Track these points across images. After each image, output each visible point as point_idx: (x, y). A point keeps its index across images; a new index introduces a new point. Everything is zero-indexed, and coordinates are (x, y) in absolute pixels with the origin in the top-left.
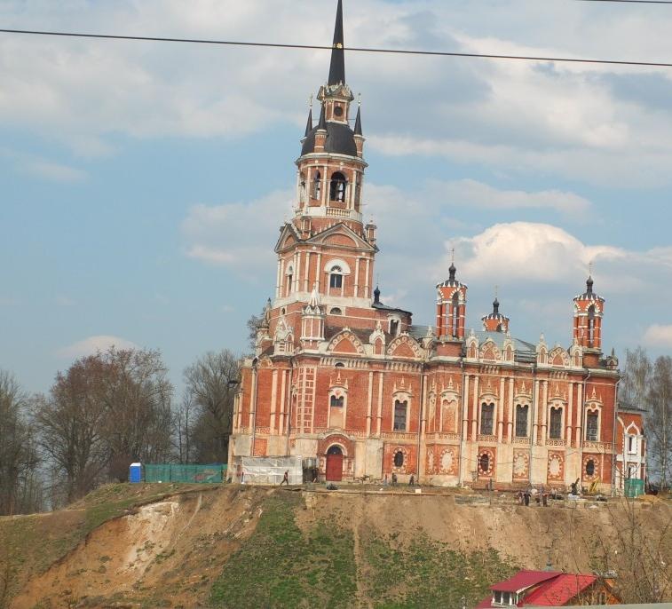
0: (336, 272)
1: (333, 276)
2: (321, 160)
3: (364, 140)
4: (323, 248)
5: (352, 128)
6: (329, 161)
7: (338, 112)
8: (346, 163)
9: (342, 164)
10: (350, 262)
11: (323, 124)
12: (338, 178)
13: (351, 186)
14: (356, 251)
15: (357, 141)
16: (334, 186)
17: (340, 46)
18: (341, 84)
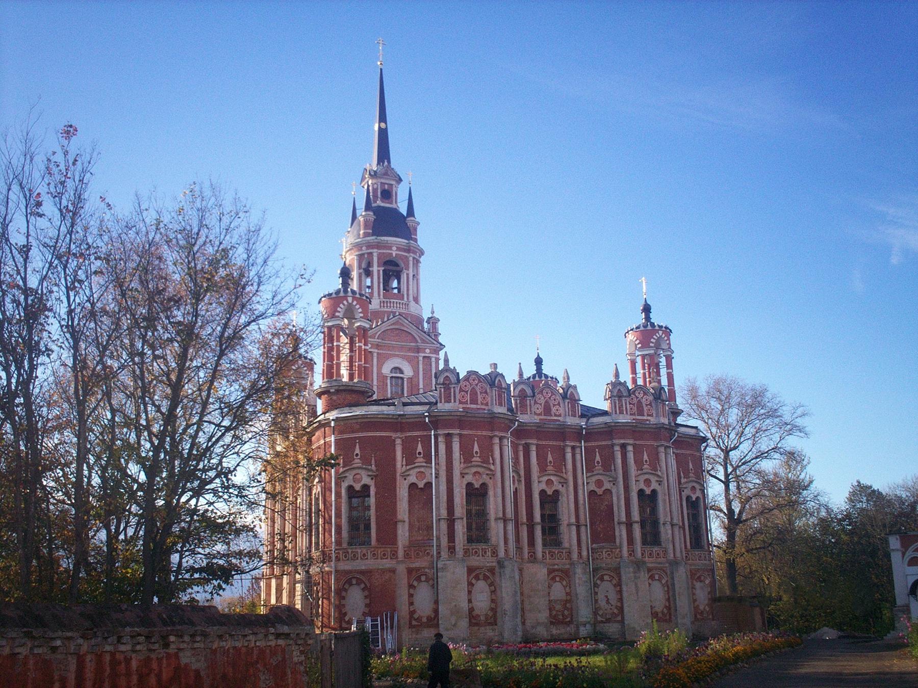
1: (392, 377)
2: (370, 246)
3: (418, 224)
4: (378, 346)
5: (405, 213)
6: (378, 246)
7: (387, 194)
8: (398, 249)
9: (394, 248)
10: (414, 362)
12: (393, 270)
13: (408, 274)
14: (418, 350)
15: (410, 224)
17: (383, 125)
18: (386, 163)
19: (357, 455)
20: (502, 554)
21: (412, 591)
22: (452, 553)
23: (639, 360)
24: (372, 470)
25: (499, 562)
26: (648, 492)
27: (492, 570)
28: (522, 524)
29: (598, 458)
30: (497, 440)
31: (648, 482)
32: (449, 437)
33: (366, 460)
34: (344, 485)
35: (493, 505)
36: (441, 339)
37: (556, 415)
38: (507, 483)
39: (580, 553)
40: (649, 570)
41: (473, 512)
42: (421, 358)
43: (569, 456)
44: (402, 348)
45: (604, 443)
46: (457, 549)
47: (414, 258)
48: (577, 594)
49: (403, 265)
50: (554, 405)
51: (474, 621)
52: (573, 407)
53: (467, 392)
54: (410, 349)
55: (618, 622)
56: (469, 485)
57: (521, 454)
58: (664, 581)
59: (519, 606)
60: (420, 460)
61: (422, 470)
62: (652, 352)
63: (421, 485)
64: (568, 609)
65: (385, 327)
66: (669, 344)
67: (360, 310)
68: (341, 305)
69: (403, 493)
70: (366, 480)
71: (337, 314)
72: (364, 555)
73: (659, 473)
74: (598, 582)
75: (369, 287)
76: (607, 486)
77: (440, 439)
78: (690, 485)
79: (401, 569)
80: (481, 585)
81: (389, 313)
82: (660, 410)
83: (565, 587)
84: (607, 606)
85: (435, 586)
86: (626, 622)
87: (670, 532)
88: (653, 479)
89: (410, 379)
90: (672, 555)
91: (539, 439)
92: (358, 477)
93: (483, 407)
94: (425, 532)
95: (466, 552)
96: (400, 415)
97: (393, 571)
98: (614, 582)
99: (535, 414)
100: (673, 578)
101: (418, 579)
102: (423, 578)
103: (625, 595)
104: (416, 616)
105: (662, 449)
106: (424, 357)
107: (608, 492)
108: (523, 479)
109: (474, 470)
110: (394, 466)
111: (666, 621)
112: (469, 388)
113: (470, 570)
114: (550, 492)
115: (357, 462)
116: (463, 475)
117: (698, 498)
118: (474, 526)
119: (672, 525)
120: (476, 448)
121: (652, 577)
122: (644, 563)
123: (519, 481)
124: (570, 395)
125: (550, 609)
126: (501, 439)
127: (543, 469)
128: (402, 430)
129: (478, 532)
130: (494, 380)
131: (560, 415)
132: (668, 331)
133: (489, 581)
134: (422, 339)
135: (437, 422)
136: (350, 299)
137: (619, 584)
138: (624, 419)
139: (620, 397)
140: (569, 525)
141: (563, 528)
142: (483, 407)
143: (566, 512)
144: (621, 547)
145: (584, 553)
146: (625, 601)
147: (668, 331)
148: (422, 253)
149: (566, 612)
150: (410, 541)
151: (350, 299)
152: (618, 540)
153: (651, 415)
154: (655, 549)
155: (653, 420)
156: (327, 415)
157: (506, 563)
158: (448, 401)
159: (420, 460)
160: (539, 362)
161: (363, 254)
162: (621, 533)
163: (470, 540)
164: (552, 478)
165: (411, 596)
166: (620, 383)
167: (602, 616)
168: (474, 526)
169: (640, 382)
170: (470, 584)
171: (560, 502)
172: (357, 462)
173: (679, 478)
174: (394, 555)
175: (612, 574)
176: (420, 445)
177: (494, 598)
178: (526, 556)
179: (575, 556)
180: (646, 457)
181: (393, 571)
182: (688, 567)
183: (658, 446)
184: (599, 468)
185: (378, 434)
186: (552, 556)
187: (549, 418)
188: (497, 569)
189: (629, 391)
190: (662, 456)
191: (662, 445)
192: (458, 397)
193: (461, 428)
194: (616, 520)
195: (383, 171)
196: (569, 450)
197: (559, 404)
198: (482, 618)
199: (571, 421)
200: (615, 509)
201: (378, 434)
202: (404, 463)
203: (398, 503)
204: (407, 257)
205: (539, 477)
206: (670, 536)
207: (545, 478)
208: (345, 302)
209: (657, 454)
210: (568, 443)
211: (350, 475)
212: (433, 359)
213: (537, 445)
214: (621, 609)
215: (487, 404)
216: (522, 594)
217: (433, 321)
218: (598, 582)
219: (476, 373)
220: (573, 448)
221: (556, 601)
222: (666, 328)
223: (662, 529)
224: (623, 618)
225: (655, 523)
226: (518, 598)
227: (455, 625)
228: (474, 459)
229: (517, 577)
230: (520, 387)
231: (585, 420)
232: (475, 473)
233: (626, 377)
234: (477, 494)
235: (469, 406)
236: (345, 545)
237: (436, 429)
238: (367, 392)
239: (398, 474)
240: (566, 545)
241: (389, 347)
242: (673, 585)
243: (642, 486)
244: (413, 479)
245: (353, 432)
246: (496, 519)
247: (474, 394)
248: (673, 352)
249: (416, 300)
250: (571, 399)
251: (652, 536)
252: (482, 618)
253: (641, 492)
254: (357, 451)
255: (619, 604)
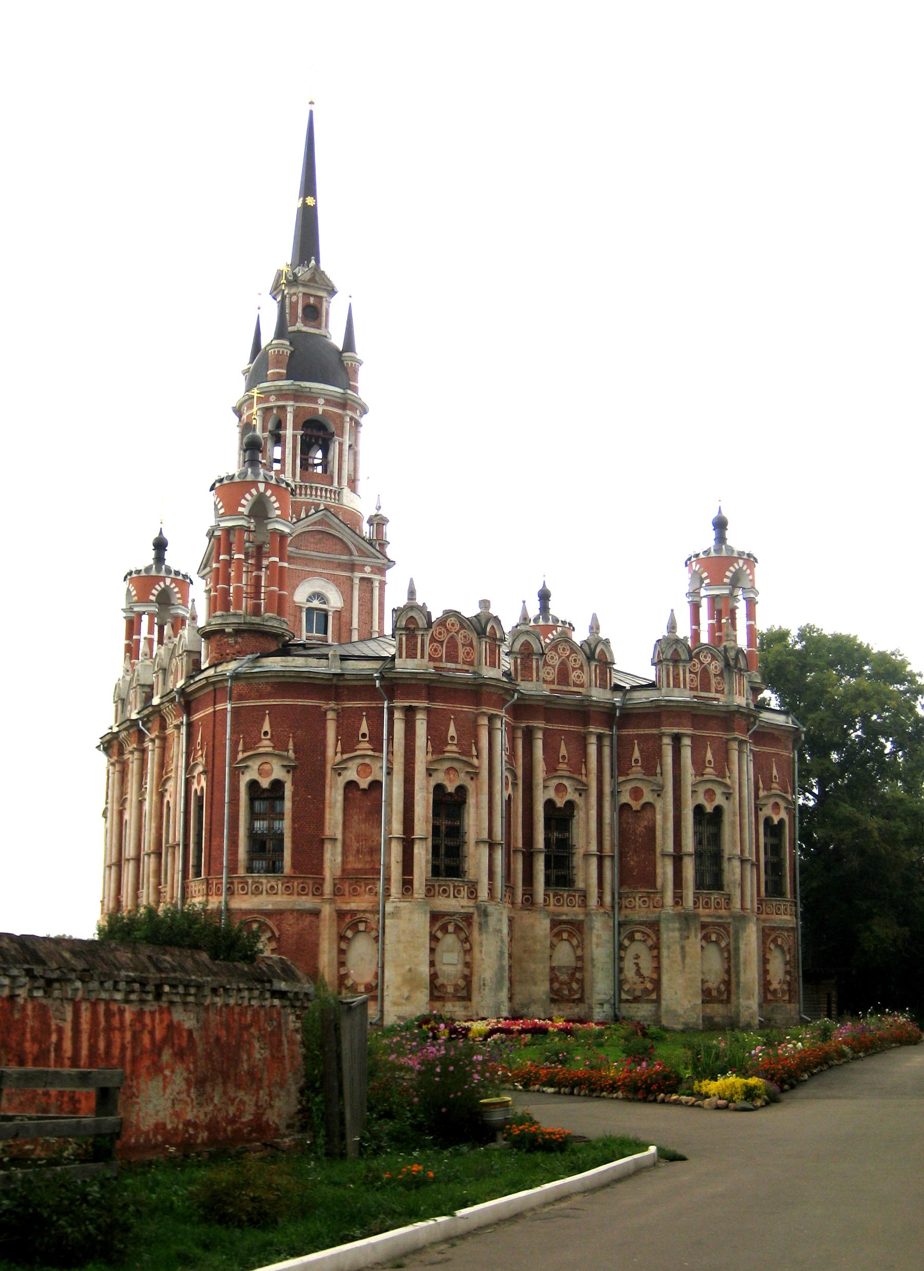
0: (316, 604)
2: (282, 394)
5: (340, 346)
6: (297, 396)
7: (314, 313)
8: (328, 402)
11: (281, 332)
12: (317, 434)
13: (341, 444)
14: (352, 567)
16: (307, 447)
17: (310, 201)
18: (313, 262)
19: (266, 733)
20: (483, 894)
21: (343, 946)
22: (407, 890)
23: (705, 603)
24: (288, 758)
25: (477, 907)
26: (709, 809)
27: (468, 918)
28: (515, 851)
29: (637, 754)
30: (484, 721)
31: (710, 794)
32: (410, 713)
33: (279, 743)
34: (245, 779)
35: (475, 821)
36: (390, 552)
37: (575, 685)
38: (498, 787)
39: (601, 897)
40: (704, 926)
41: (443, 828)
42: (357, 581)
43: (593, 749)
44: (328, 563)
45: (648, 731)
46: (416, 884)
47: (352, 419)
48: (592, 959)
49: (333, 428)
50: (574, 669)
51: (436, 994)
52: (603, 674)
53: (441, 643)
54: (340, 565)
55: (653, 1001)
56: (439, 788)
57: (520, 743)
58: (723, 944)
59: (506, 974)
60: (364, 746)
61: (367, 761)
62: (727, 592)
63: (364, 784)
64: (577, 981)
65: (301, 527)
66: (753, 581)
67: (277, 505)
68: (248, 496)
69: (335, 796)
70: (278, 772)
71: (240, 509)
72: (272, 887)
73: (728, 781)
74: (626, 943)
75: (277, 461)
76: (648, 797)
77: (398, 715)
78: (772, 801)
79: (327, 910)
80: (450, 940)
81: (308, 505)
82: (736, 687)
83: (574, 948)
84: (637, 979)
85: (379, 939)
86: (663, 1002)
87: (738, 871)
88: (719, 791)
89: (338, 613)
90: (738, 906)
91: (548, 721)
92: (266, 767)
93: (466, 667)
94: (368, 858)
95: (429, 891)
96: (334, 674)
97: (316, 913)
98: (650, 942)
99: (545, 681)
100: (737, 940)
101: (354, 927)
102: (362, 927)
103: (665, 962)
104: (349, 982)
105: (735, 745)
106: (362, 579)
107: (648, 806)
108: (520, 782)
109: (447, 765)
110: (324, 753)
111: (721, 1002)
112: (445, 638)
113: (435, 917)
114: (560, 803)
115: (266, 745)
116: (430, 772)
117: (781, 821)
118: (443, 850)
119: (743, 861)
120: (452, 731)
121: (706, 938)
122: (696, 916)
123: (515, 785)
124: (597, 655)
125: (552, 981)
126: (491, 718)
127: (552, 769)
128: (338, 698)
129: (449, 862)
130: (483, 626)
131: (582, 686)
132: (751, 560)
133: (462, 935)
134: (359, 550)
135: (393, 685)
136: (262, 487)
137: (656, 947)
138: (681, 695)
139: (676, 661)
140: (587, 855)
141: (578, 860)
142: (466, 667)
143: (584, 834)
144: (662, 892)
145: (608, 899)
146: (664, 971)
147: (751, 560)
148: (364, 411)
149: (575, 986)
150: (343, 870)
151: (262, 487)
152: (659, 881)
153: (722, 692)
154: (715, 896)
155: (723, 699)
156: (219, 669)
157: (491, 909)
158: (412, 655)
159: (364, 746)
160: (544, 596)
161: (271, 408)
162: (665, 870)
163: (436, 871)
164: (566, 782)
165: (342, 952)
166: (678, 641)
167: (627, 992)
168: (443, 850)
169: (704, 638)
170: (434, 938)
171: (574, 821)
172: (266, 745)
173: (757, 789)
174: (318, 891)
175: (648, 931)
176: (364, 722)
177: (468, 959)
178: (519, 898)
179: (593, 901)
180: (709, 756)
181: (316, 913)
182: (762, 924)
183: (728, 740)
184: (637, 771)
185: (300, 702)
186: (558, 900)
187: (565, 688)
188: (475, 916)
189: (690, 651)
190: (735, 755)
191: (735, 739)
192: (427, 650)
193: (431, 699)
194: (658, 850)
195: (307, 276)
196: (593, 739)
197: (581, 668)
198: (450, 989)
199: (598, 695)
200: (659, 833)
201: (300, 702)
202: (339, 749)
203: (327, 810)
204: (341, 417)
205: (545, 781)
206: (738, 876)
207: (554, 782)
208: (254, 491)
209: (727, 752)
210: (592, 729)
211: (255, 765)
212: (376, 584)
213: (545, 731)
214: (657, 983)
215: (471, 664)
216: (510, 956)
217: (379, 522)
218: (626, 943)
219: (456, 614)
220: (600, 737)
221: (560, 968)
222: (749, 555)
223: (726, 865)
224: (659, 996)
225: (717, 858)
226: (506, 962)
227: (408, 998)
228: (449, 748)
229: (505, 930)
230: (522, 639)
231: (620, 694)
232: (449, 769)
233: (684, 631)
234: (449, 805)
235: (444, 665)
236: (242, 872)
237: (391, 700)
238: (283, 635)
239: (329, 767)
240: (580, 885)
241: (308, 561)
242: (737, 949)
243: (701, 799)
244: (351, 774)
245: (261, 697)
246: (478, 843)
247: (452, 644)
248: (757, 593)
249: (353, 484)
250: (599, 661)
251: (711, 877)
252: (450, 989)
253: (699, 809)
254: (266, 727)
255: (655, 976)
